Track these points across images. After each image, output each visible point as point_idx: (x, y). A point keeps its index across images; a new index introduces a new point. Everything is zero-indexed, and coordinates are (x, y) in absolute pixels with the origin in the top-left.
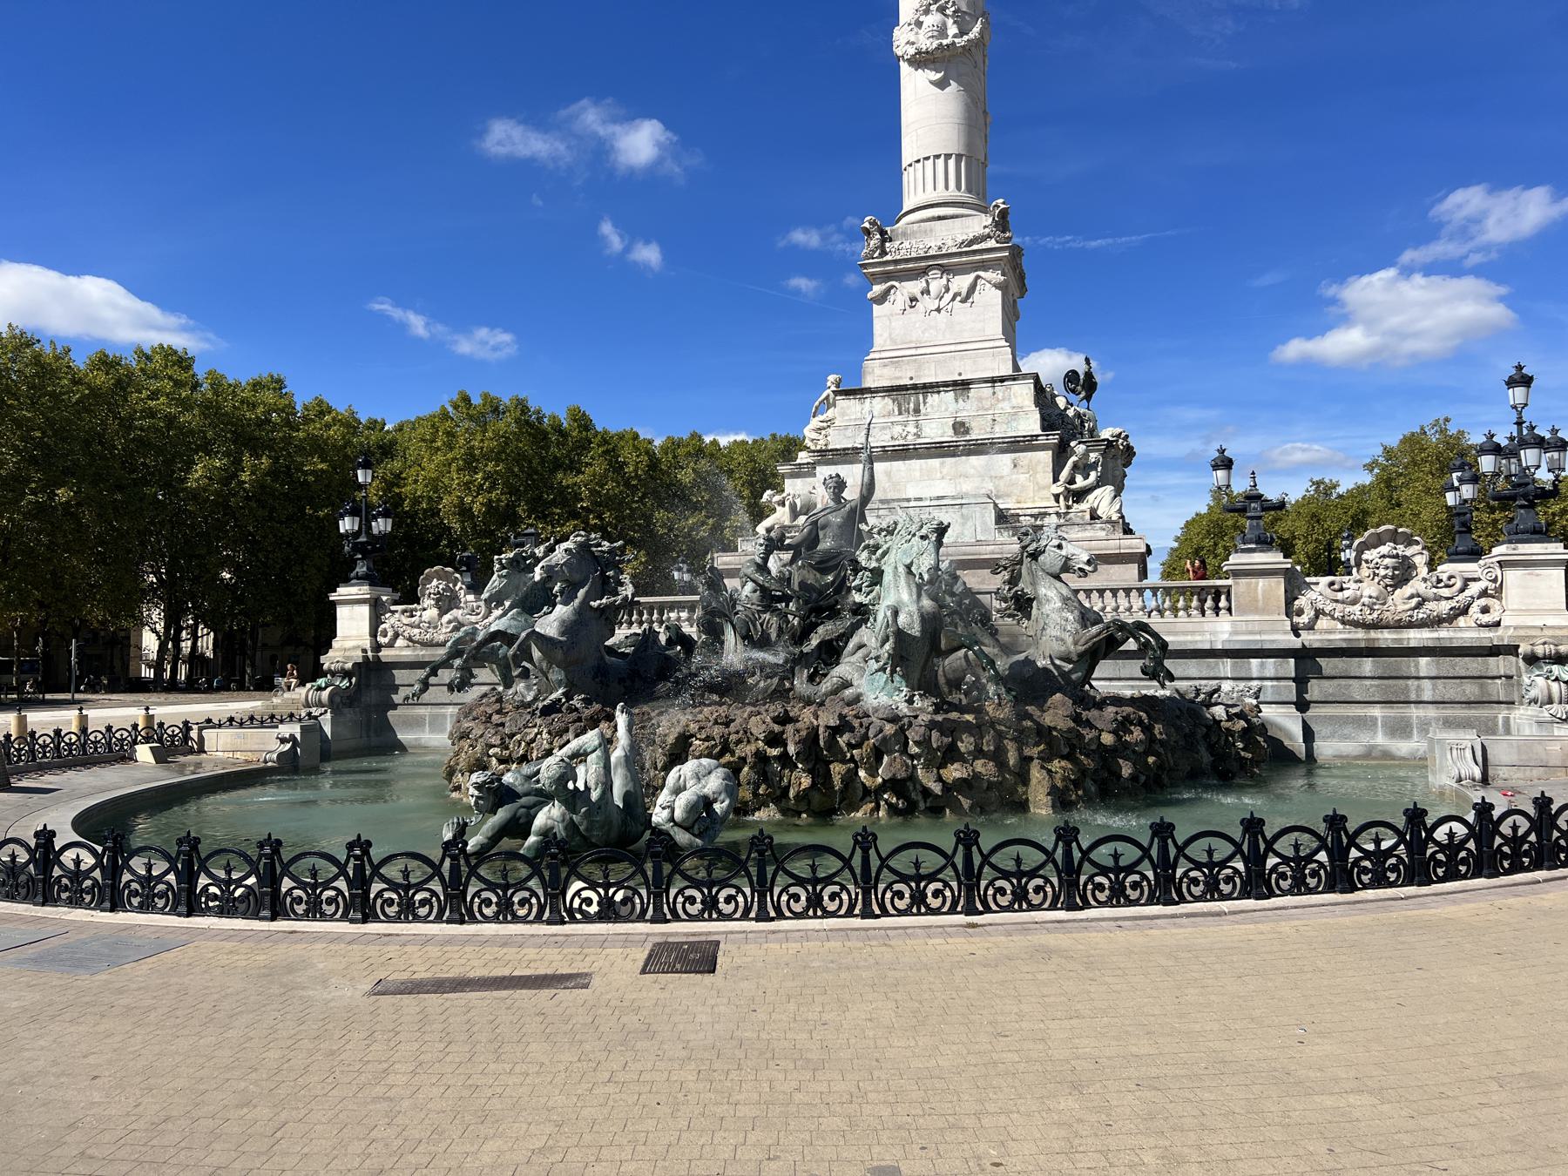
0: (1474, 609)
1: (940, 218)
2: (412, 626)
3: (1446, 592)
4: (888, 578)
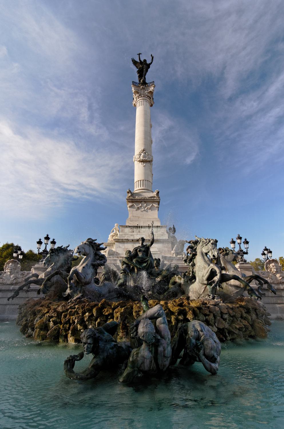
1: (144, 192)
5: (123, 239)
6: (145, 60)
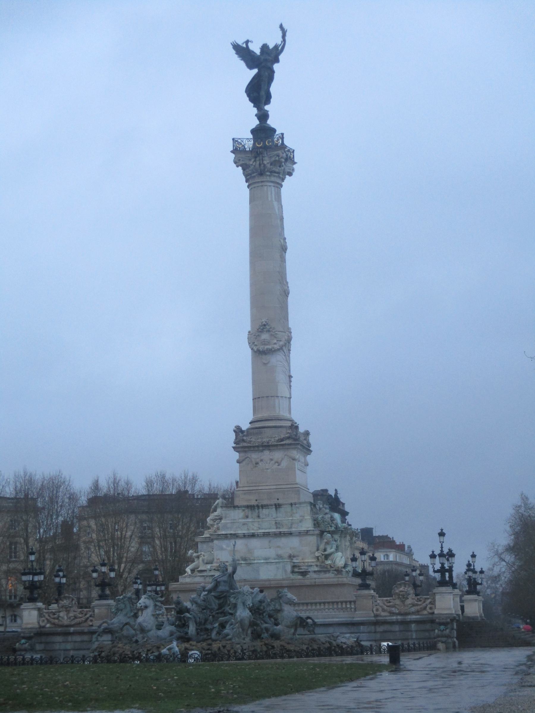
0: (428, 608)
2: (54, 618)
3: (419, 603)
4: (238, 606)
5: (226, 534)
6: (265, 48)
